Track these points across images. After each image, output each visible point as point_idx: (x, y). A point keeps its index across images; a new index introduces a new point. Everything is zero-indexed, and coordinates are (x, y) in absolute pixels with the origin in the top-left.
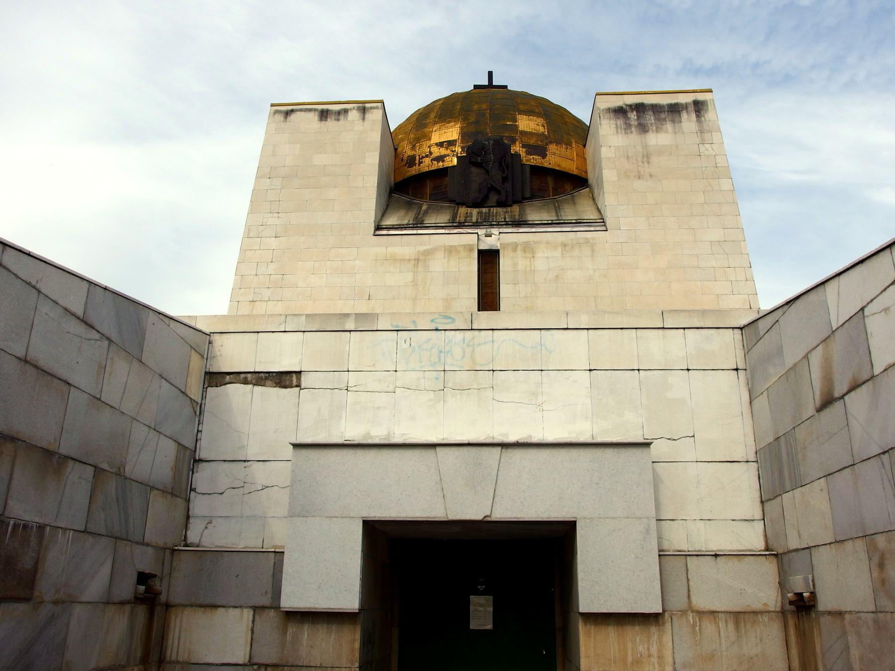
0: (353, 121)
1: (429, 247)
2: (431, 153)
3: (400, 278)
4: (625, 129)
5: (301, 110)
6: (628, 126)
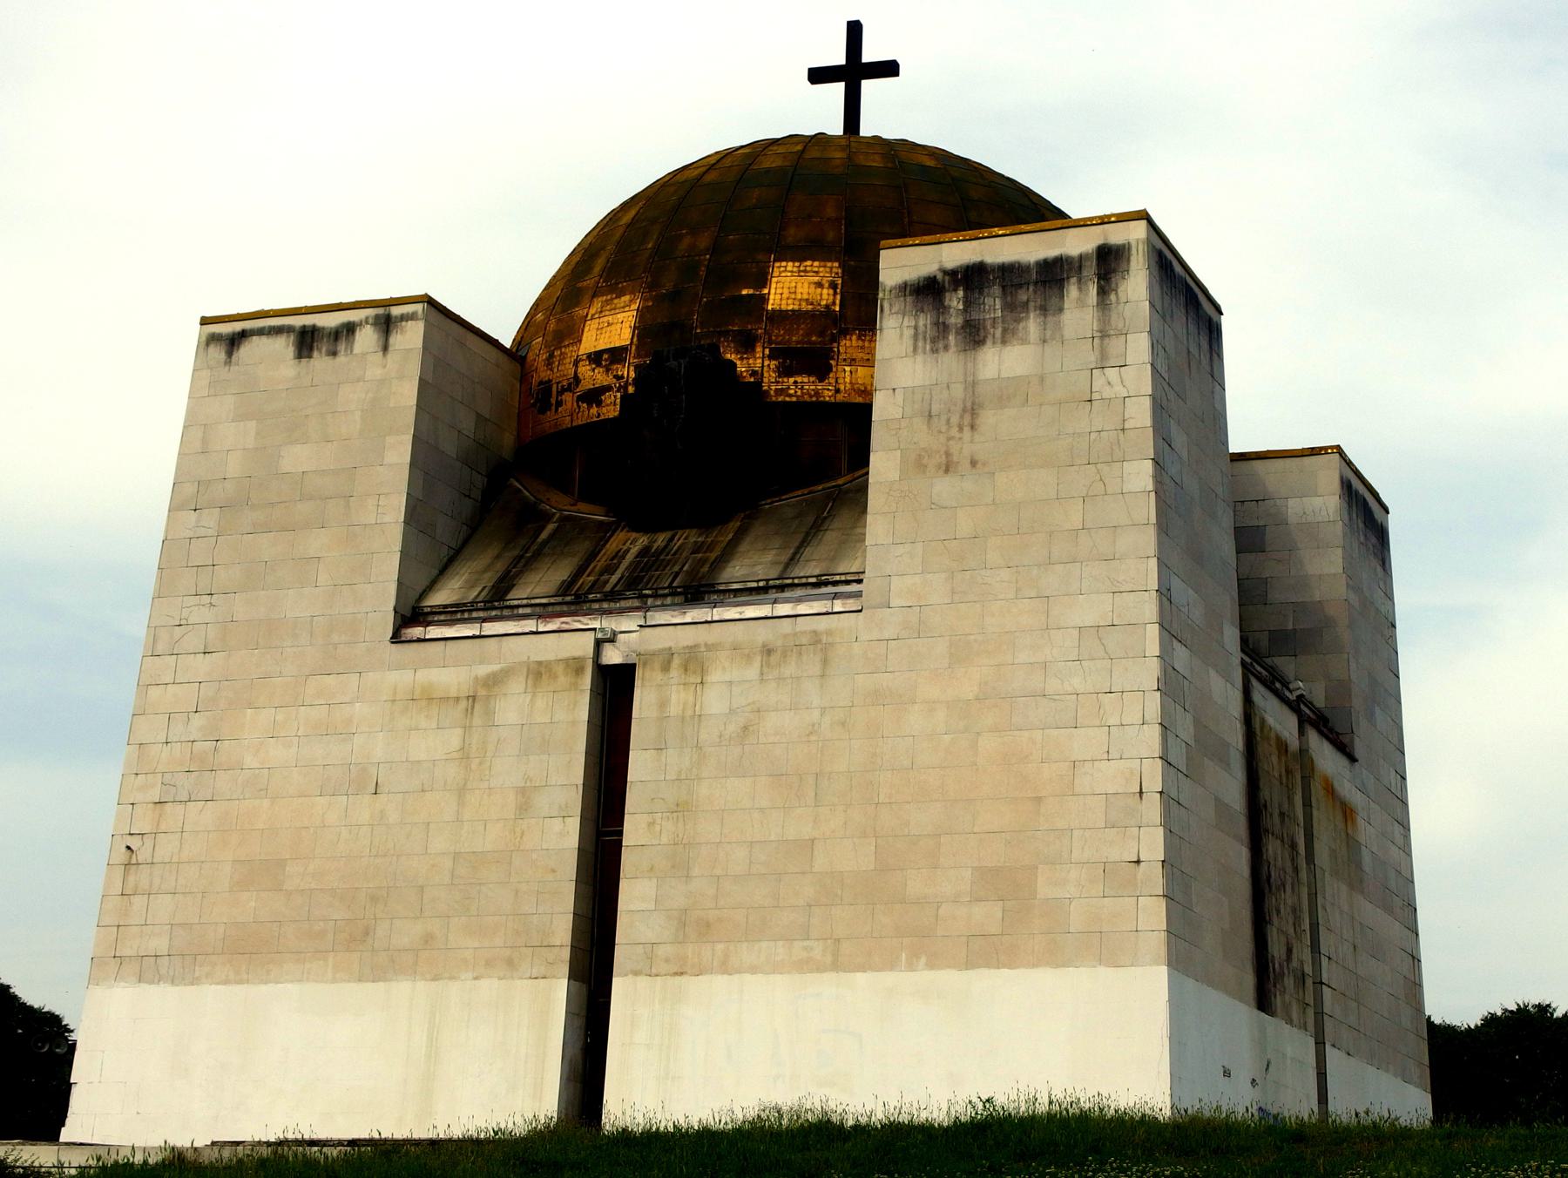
0: (364, 354)
1: (496, 667)
2: (577, 379)
3: (434, 742)
4: (934, 341)
5: (261, 332)
6: (942, 329)
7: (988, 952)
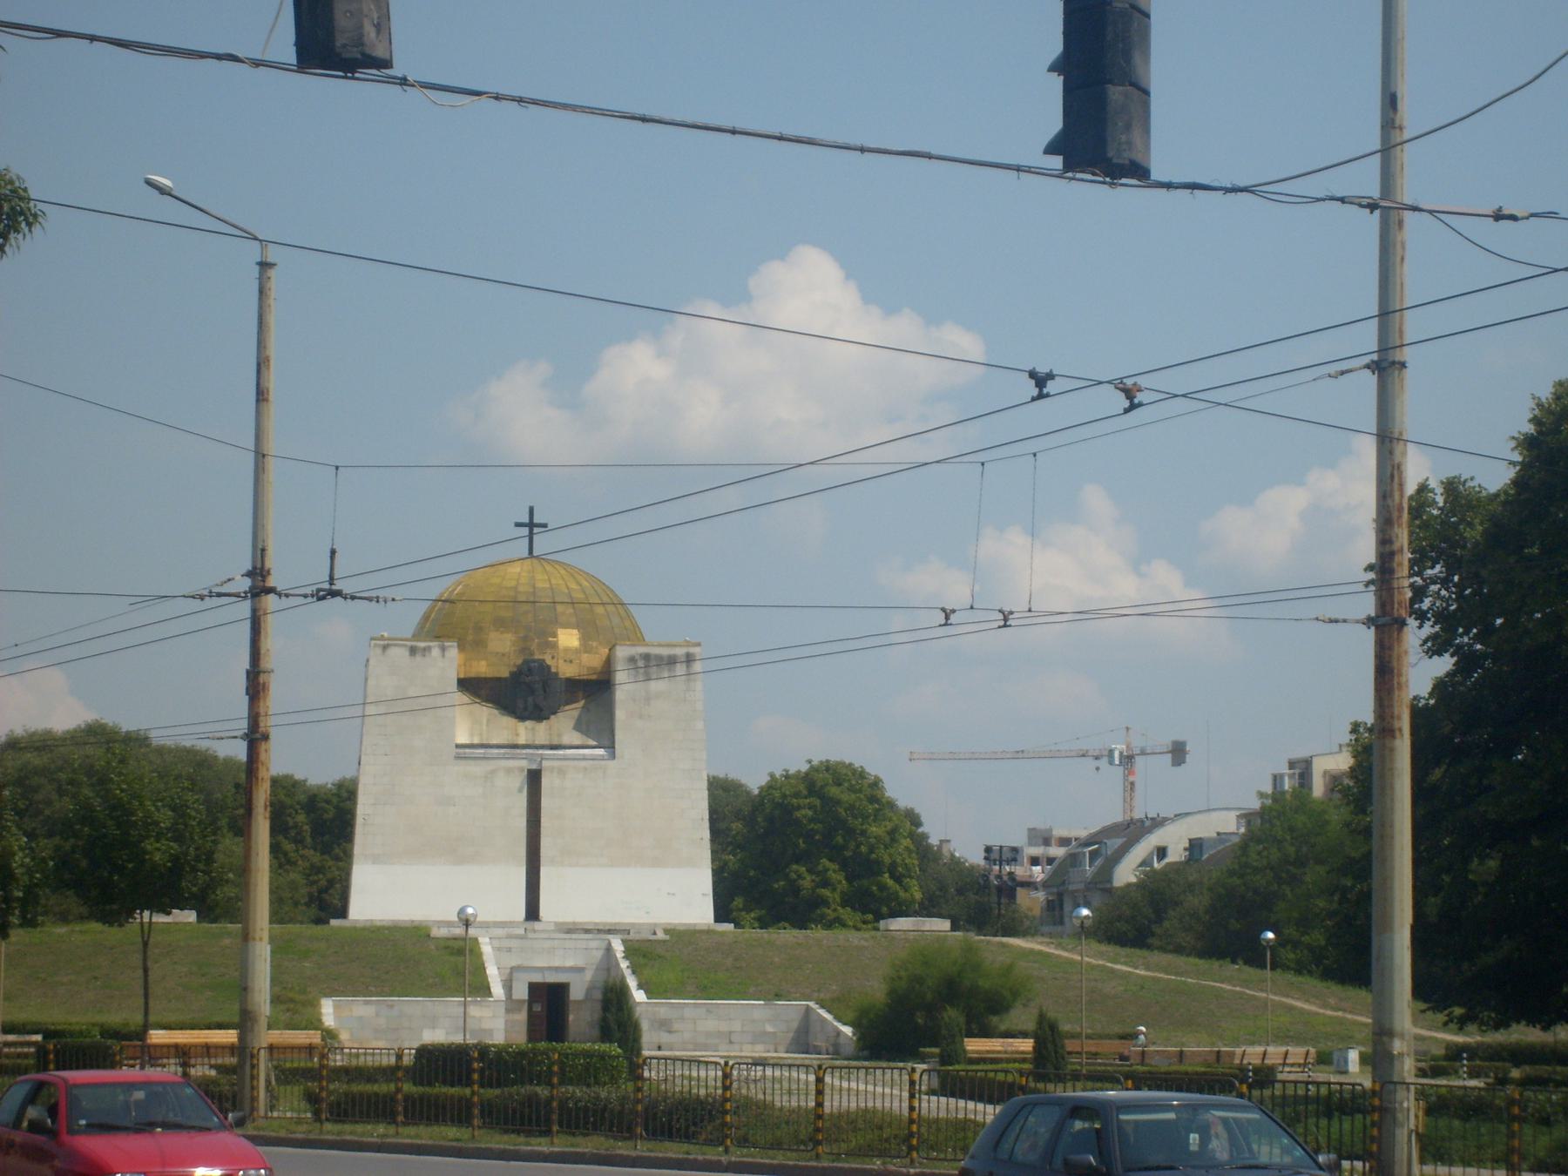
7: (657, 863)
